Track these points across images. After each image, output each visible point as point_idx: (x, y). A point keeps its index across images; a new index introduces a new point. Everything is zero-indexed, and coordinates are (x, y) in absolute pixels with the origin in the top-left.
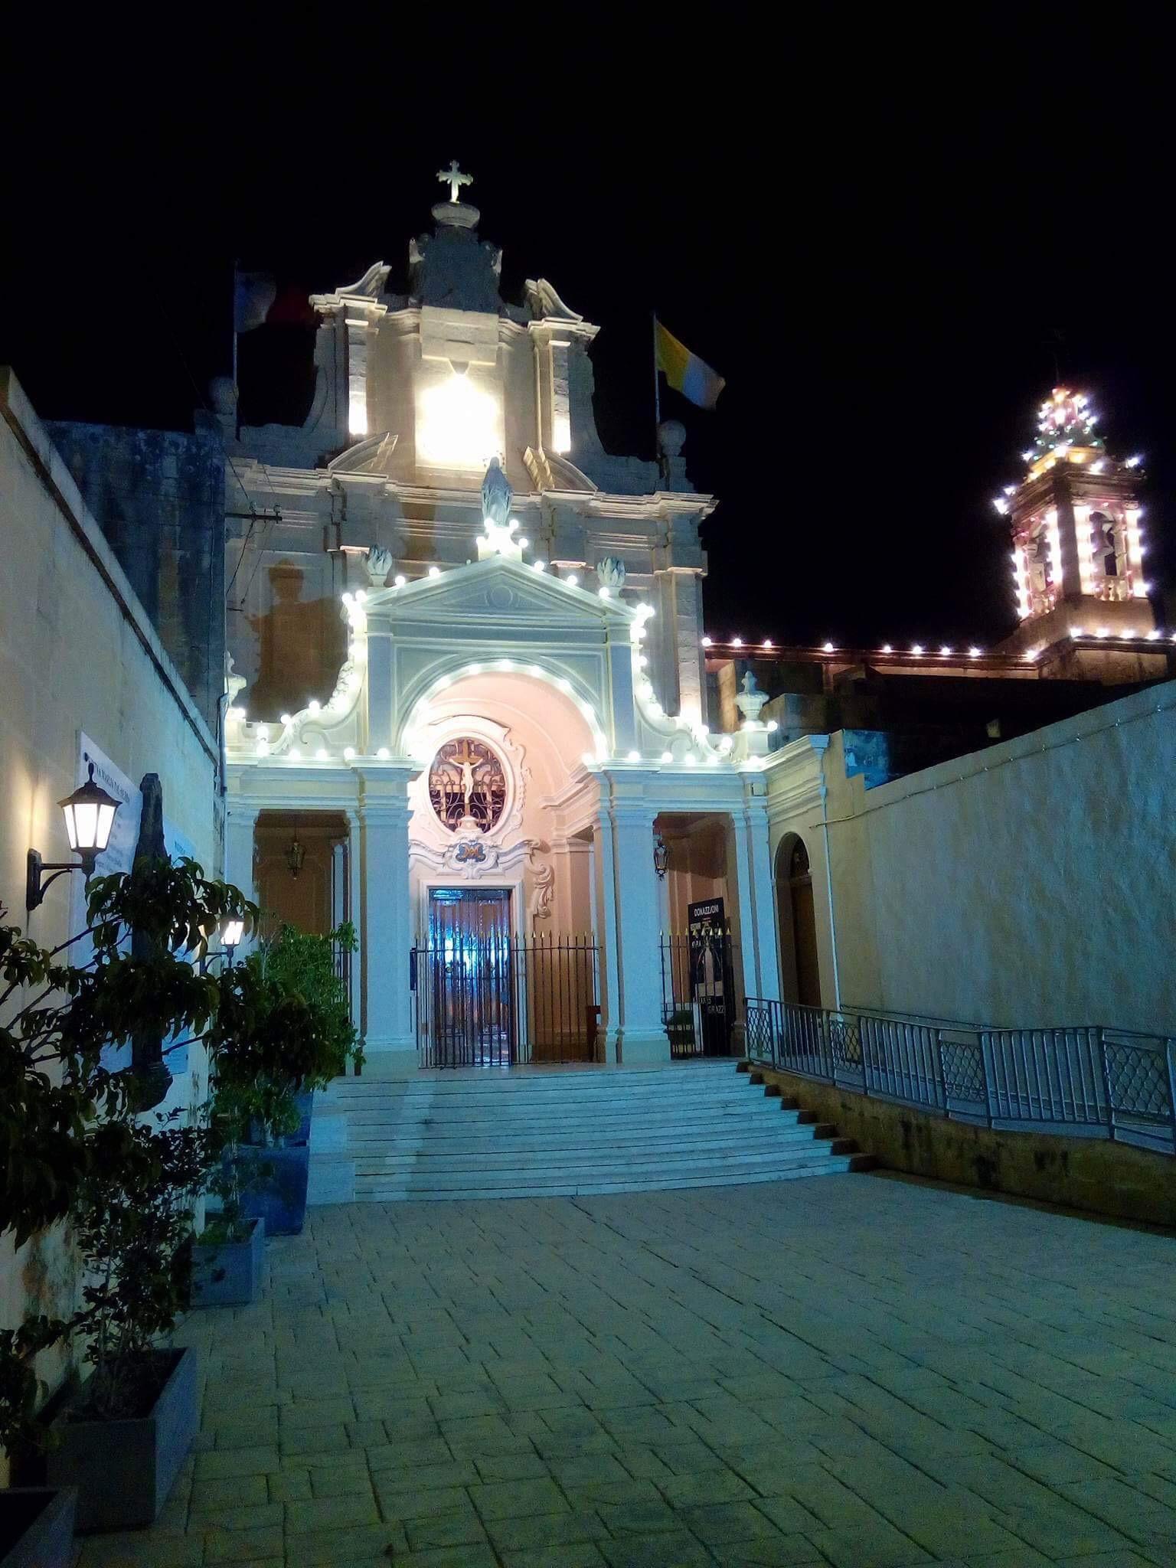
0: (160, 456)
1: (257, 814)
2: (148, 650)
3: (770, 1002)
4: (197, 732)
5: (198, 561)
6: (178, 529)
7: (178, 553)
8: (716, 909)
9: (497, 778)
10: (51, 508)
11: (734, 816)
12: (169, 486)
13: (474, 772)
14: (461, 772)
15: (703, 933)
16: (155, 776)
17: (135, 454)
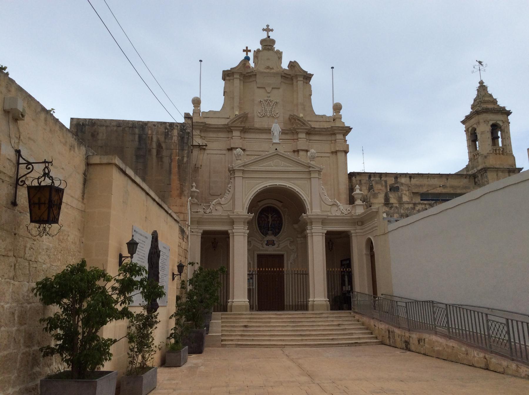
0: (172, 130)
1: (202, 231)
2: (154, 200)
3: (357, 292)
4: (171, 216)
5: (183, 160)
6: (178, 150)
7: (177, 158)
8: (348, 262)
10: (126, 178)
11: (352, 232)
12: (175, 139)
14: (268, 217)
15: (344, 270)
16: (156, 231)
17: (166, 129)
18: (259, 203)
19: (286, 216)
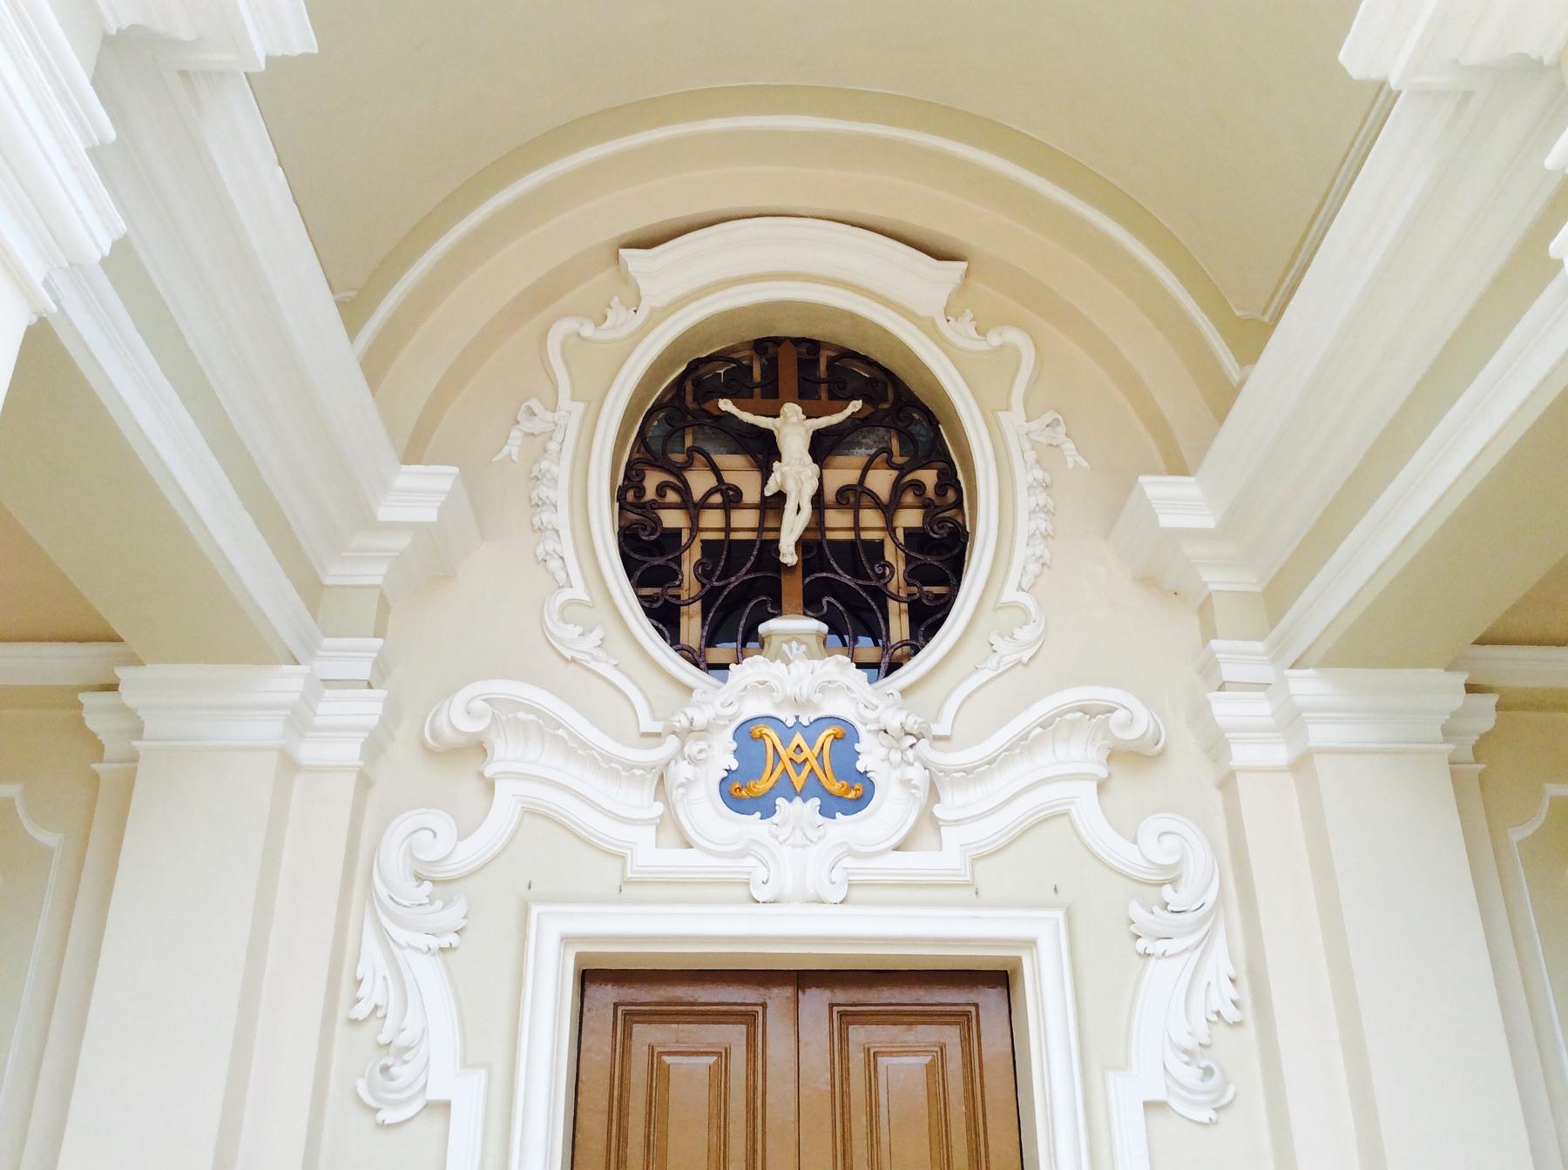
9: (929, 477)
13: (823, 448)
14: (764, 451)
18: (634, 259)
19: (1013, 420)
